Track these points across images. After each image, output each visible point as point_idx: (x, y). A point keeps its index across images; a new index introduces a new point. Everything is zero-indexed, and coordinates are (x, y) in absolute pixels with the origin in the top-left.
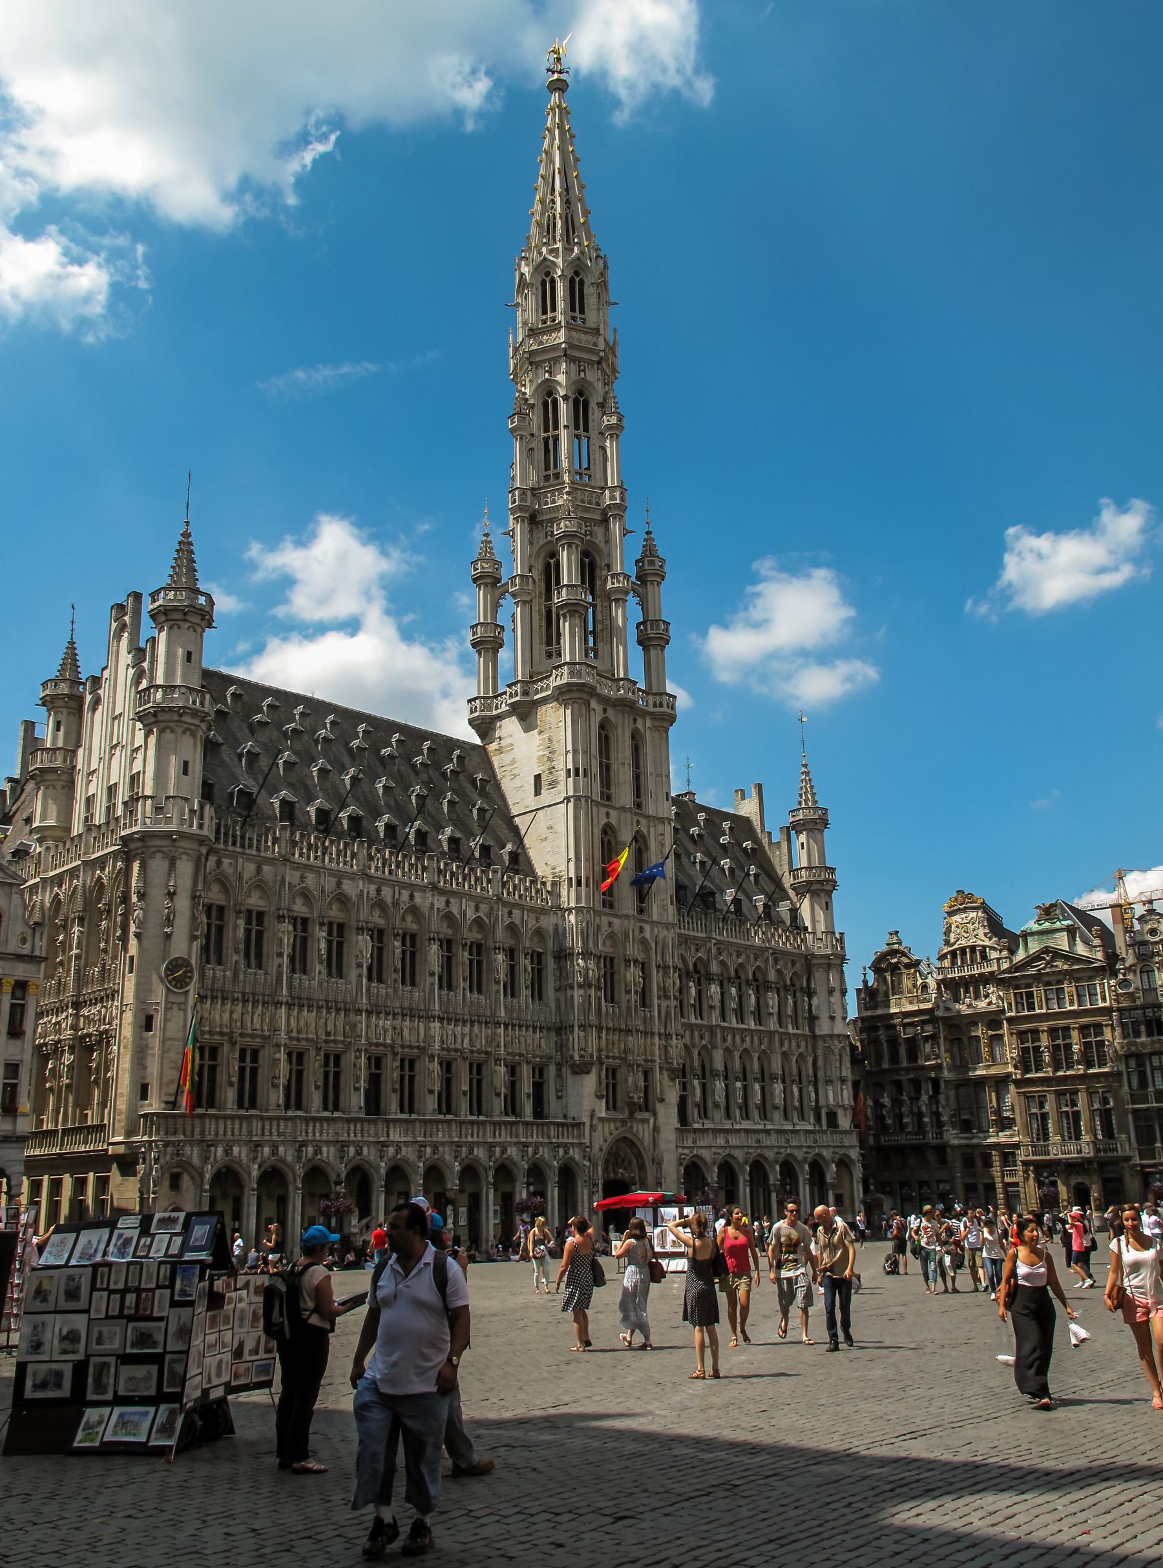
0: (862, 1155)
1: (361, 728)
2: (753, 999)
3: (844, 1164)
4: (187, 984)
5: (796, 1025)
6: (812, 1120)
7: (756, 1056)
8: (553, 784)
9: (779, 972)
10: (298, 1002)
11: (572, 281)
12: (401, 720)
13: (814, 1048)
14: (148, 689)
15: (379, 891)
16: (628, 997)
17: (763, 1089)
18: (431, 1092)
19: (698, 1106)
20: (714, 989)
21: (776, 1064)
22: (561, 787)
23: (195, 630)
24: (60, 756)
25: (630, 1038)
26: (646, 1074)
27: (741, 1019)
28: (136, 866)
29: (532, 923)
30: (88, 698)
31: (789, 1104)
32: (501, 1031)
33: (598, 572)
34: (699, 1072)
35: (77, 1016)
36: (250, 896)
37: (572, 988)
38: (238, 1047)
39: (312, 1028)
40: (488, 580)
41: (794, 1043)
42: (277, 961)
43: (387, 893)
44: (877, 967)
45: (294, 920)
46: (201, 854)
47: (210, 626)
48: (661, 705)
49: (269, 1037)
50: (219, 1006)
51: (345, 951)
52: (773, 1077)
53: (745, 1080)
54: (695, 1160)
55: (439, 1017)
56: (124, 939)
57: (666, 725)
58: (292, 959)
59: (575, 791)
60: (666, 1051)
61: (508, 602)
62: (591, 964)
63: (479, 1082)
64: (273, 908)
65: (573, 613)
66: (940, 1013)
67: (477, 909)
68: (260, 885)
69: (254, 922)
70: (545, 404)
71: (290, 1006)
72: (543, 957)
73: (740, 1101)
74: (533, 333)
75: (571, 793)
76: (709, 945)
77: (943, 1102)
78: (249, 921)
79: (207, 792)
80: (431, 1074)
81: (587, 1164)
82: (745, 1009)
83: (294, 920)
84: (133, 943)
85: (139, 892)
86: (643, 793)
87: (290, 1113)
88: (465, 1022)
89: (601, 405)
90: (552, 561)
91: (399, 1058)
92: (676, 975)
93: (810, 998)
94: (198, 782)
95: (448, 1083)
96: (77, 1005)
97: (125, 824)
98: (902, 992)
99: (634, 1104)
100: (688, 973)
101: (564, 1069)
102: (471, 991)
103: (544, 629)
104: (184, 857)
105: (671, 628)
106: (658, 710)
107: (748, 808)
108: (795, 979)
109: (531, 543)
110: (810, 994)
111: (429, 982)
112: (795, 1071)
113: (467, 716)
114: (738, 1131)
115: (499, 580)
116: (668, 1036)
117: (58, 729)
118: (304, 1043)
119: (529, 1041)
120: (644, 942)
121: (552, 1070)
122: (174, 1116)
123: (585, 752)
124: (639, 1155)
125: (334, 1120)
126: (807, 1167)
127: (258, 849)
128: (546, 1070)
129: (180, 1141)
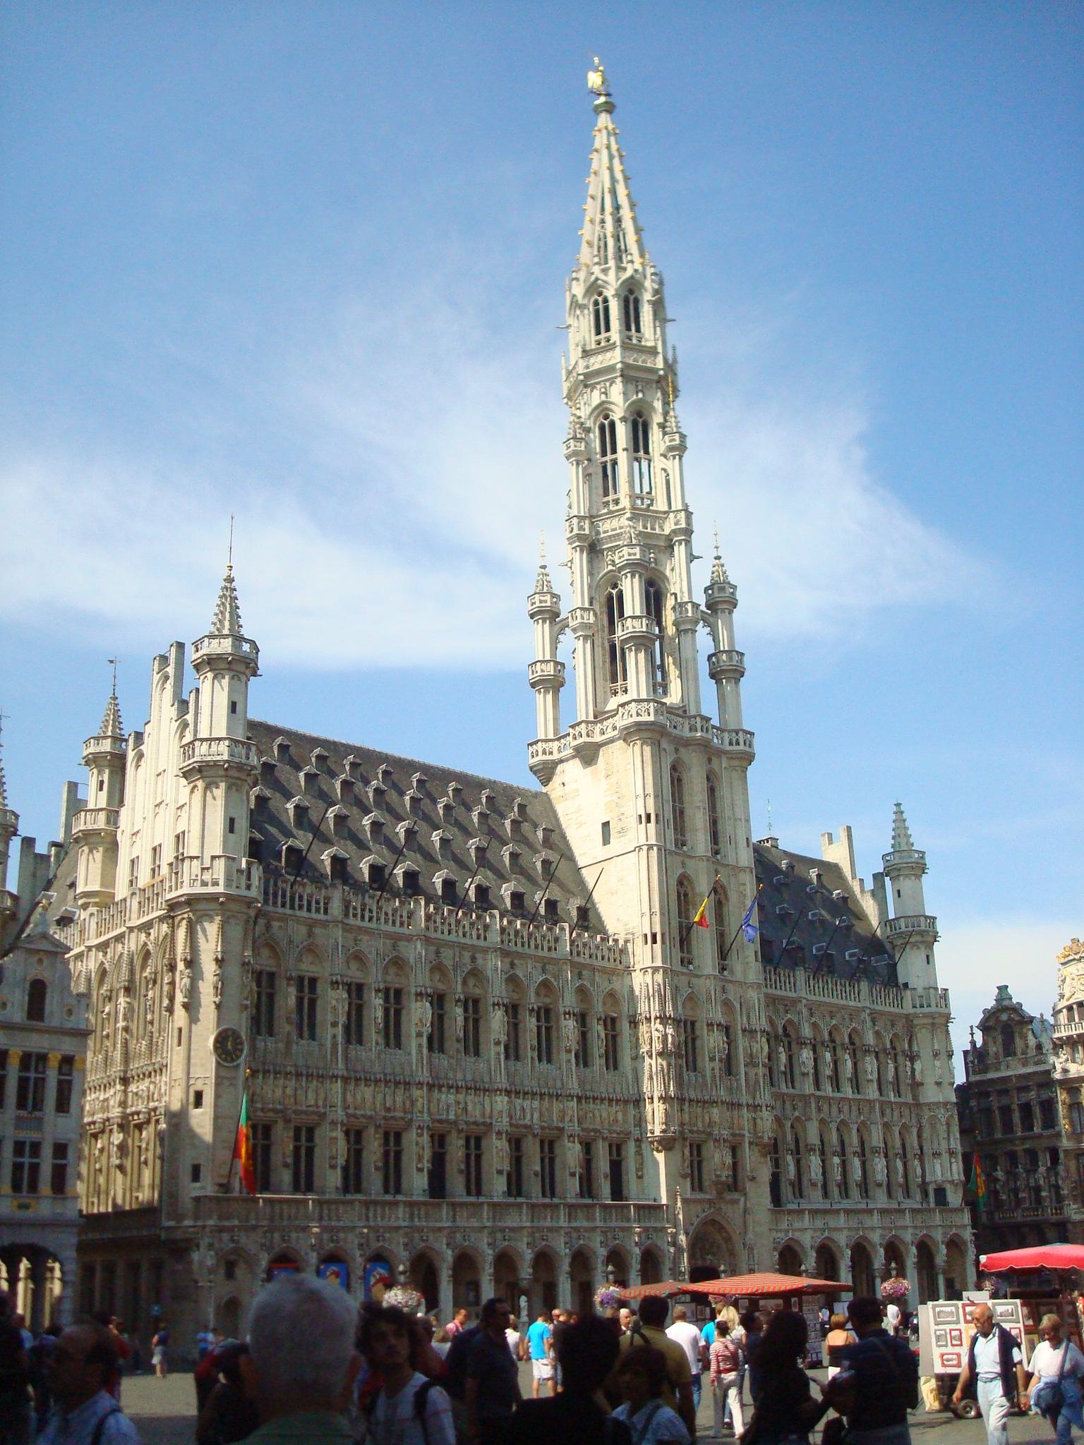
0: (974, 1234)
1: (453, 785)
2: (849, 1064)
3: (955, 1245)
4: (238, 1057)
5: (898, 1093)
6: (918, 1197)
7: (855, 1127)
8: (622, 831)
9: (877, 1034)
10: (352, 1078)
12: (458, 769)
13: (919, 1117)
14: (192, 743)
15: (438, 953)
16: (712, 1064)
17: (863, 1164)
18: (500, 1172)
19: (792, 1184)
20: (806, 1055)
21: (876, 1137)
22: (631, 834)
23: (239, 680)
24: (102, 816)
25: (715, 1110)
26: (734, 1150)
27: (837, 1086)
28: (181, 933)
30: (131, 755)
31: (892, 1179)
34: (792, 1146)
35: (125, 1092)
36: (301, 960)
37: (651, 1057)
38: (292, 1125)
39: (368, 1104)
41: (896, 1113)
42: (330, 1031)
43: (447, 957)
44: (985, 1027)
45: (348, 987)
46: (250, 917)
47: (255, 674)
48: (738, 743)
49: (325, 1113)
51: (404, 1018)
52: (875, 1151)
53: (843, 1153)
54: (792, 1244)
55: (506, 1090)
56: (170, 1010)
57: (744, 763)
58: (347, 1028)
60: (755, 1124)
61: (568, 639)
62: (670, 1031)
63: (552, 1160)
64: (327, 974)
66: (1057, 1075)
67: (544, 971)
68: (310, 949)
69: (306, 990)
70: (602, 428)
71: (346, 1080)
72: (618, 1021)
73: (839, 1178)
74: (586, 353)
75: (643, 841)
76: (799, 1004)
77: (1062, 1173)
78: (300, 989)
79: (256, 850)
80: (497, 1152)
81: (672, 1250)
82: (841, 1076)
83: (348, 987)
84: (180, 1013)
85: (185, 960)
86: (720, 840)
87: (349, 1197)
89: (662, 426)
90: (614, 592)
91: (463, 1135)
92: (764, 1040)
93: (912, 1064)
94: (244, 842)
95: (517, 1160)
96: (125, 1081)
97: (171, 887)
98: (1015, 1054)
99: (722, 1183)
100: (777, 1037)
101: (643, 1146)
102: (540, 1060)
103: (608, 665)
105: (745, 658)
106: (737, 748)
107: (835, 854)
108: (895, 1041)
109: (591, 574)
110: (912, 1059)
111: (493, 1054)
112: (898, 1143)
114: (837, 1211)
115: (558, 615)
116: (756, 1107)
117: (101, 789)
118: (363, 1120)
119: (605, 1115)
120: (727, 1004)
121: (631, 1147)
122: (228, 1200)
123: (656, 797)
124: (728, 1240)
125: (396, 1204)
126: (914, 1250)
127: (309, 910)
128: (624, 1147)
129: (234, 1227)
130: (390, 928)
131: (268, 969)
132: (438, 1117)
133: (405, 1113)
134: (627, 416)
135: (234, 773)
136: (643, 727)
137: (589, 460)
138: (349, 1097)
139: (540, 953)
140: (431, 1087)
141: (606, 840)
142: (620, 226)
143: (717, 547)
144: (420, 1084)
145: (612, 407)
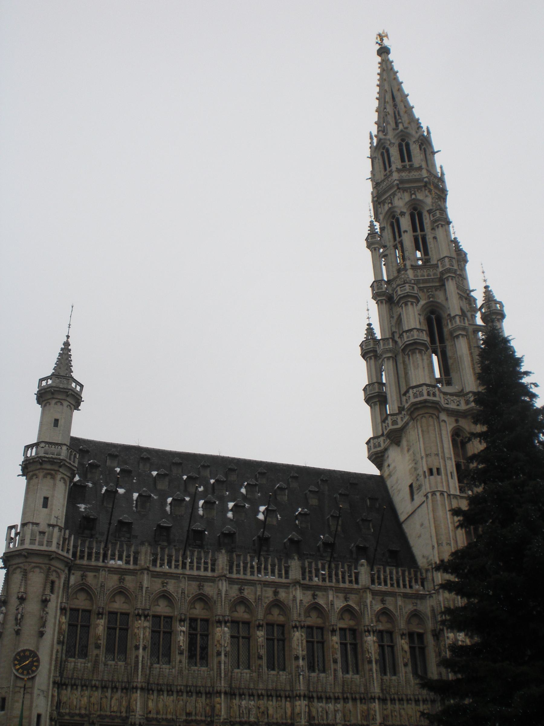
4: (33, 672)
8: (420, 487)
11: (400, 145)
23: (62, 404)
29: (409, 607)
32: (376, 706)
33: (444, 322)
40: (372, 354)
50: (79, 693)
59: (430, 487)
65: (413, 352)
67: (346, 599)
70: (392, 225)
75: (428, 490)
88: (337, 699)
102: (346, 671)
104: (37, 570)
113: (366, 454)
123: (437, 455)
130: (195, 573)
131: (83, 608)
132: (238, 720)
133: (206, 716)
134: (405, 210)
135: (48, 467)
136: (419, 406)
137: (384, 247)
138: (151, 704)
139: (342, 585)
140: (231, 694)
141: (412, 499)
142: (395, 108)
143: (485, 281)
144: (219, 693)
145: (396, 209)
